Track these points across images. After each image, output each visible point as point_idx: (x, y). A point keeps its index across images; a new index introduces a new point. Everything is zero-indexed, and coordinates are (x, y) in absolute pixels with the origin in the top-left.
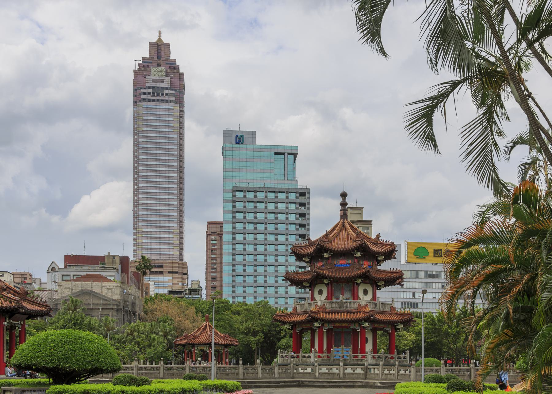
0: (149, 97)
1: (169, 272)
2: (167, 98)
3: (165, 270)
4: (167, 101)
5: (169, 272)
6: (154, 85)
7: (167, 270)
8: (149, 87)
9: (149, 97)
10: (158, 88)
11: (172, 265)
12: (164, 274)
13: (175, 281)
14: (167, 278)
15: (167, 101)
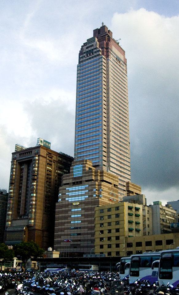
0: (84, 59)
1: (87, 181)
2: (95, 54)
3: (83, 180)
4: (95, 56)
5: (87, 181)
6: (87, 50)
7: (84, 180)
8: (85, 53)
9: (84, 59)
10: (90, 50)
11: (88, 174)
12: (83, 183)
13: (90, 188)
14: (84, 186)
15: (95, 56)
